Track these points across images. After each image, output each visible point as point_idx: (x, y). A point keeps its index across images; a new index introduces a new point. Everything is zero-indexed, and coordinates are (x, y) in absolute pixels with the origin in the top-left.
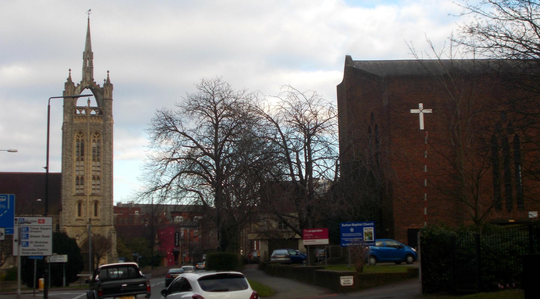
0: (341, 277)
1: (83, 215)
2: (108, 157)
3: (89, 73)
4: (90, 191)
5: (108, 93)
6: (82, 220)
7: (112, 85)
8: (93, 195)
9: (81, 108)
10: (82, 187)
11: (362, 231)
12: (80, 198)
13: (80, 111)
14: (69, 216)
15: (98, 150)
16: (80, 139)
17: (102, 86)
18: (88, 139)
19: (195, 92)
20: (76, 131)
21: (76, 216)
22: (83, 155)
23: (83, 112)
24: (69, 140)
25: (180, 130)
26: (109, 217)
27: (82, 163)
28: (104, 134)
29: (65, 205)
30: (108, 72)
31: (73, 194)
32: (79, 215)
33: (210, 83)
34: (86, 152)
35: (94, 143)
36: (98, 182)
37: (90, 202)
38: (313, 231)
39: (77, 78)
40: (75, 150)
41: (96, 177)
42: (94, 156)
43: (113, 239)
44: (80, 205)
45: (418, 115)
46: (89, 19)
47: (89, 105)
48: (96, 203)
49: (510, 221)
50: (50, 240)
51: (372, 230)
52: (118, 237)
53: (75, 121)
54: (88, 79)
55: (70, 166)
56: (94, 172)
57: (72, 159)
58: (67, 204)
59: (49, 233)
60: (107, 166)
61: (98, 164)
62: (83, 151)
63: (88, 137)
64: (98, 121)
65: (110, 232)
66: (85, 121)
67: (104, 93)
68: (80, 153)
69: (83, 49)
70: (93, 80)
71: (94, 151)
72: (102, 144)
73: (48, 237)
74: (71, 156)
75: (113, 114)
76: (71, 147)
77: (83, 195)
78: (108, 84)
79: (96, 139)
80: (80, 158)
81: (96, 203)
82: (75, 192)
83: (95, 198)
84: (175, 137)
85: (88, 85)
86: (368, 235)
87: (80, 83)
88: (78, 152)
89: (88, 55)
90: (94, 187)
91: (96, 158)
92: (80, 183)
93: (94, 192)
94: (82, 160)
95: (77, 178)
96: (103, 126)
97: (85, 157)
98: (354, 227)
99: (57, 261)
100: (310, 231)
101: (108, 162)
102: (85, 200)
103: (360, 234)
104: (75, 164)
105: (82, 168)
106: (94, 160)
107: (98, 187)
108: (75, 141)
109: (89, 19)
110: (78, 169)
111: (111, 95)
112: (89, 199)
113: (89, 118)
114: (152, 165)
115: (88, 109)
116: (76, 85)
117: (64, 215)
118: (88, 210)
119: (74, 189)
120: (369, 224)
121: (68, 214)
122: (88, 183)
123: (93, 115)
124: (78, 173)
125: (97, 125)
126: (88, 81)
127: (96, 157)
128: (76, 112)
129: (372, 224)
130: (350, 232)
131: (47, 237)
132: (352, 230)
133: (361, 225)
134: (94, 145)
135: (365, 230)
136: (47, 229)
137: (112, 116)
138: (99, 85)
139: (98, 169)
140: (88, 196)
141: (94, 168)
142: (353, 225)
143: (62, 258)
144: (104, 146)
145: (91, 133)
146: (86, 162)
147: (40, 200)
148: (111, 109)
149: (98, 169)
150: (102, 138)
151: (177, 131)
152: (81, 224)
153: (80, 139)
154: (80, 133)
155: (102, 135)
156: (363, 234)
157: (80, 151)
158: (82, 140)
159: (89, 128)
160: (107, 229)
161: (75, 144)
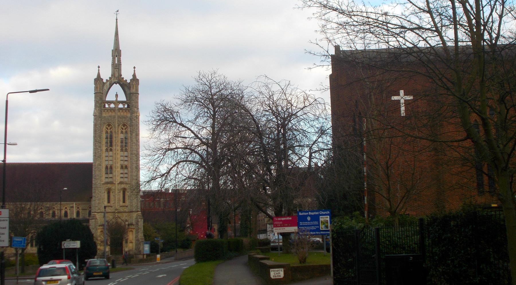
0: (271, 270)
1: (112, 202)
2: (134, 147)
4: (118, 179)
5: (135, 88)
6: (111, 207)
7: (138, 80)
8: (121, 183)
9: (110, 102)
10: (111, 176)
11: (318, 220)
12: (109, 186)
13: (109, 105)
14: (99, 203)
15: (125, 141)
16: (109, 131)
17: (129, 81)
18: (117, 131)
19: (193, 84)
20: (104, 123)
21: (106, 203)
22: (111, 145)
23: (112, 106)
25: (179, 121)
26: (135, 203)
27: (111, 153)
28: (131, 126)
29: (95, 192)
30: (134, 68)
31: (103, 183)
32: (109, 202)
33: (207, 75)
34: (114, 144)
35: (122, 135)
36: (126, 171)
37: (118, 190)
38: (283, 219)
39: (106, 74)
40: (104, 141)
41: (124, 166)
42: (122, 146)
43: (139, 224)
44: (109, 193)
45: (399, 101)
46: (117, 19)
47: (117, 99)
48: (124, 190)
49: (493, 205)
50: (6, 231)
51: (328, 218)
52: (144, 222)
53: (104, 115)
54: (117, 75)
55: (100, 157)
56: (122, 162)
57: (101, 150)
58: (97, 192)
59: (6, 224)
60: (134, 155)
61: (126, 154)
62: (111, 142)
63: (117, 129)
64: (125, 114)
65: (137, 218)
66: (113, 114)
67: (131, 88)
68: (109, 144)
69: (112, 47)
70: (121, 75)
71: (122, 142)
72: (129, 135)
73: (5, 228)
74: (100, 147)
75: (139, 107)
77: (112, 183)
78: (135, 79)
79: (124, 131)
81: (124, 190)
82: (104, 180)
83: (123, 186)
84: (175, 129)
85: (117, 80)
86: (324, 224)
87: (108, 79)
88: (107, 143)
89: (117, 53)
90: (122, 176)
91: (124, 149)
92: (109, 172)
93: (122, 180)
94: (111, 150)
95: (107, 168)
96: (131, 119)
97: (114, 148)
98: (311, 216)
99: (71, 247)
100: (279, 219)
101: (135, 152)
102: (113, 187)
103: (316, 223)
104: (104, 154)
105: (111, 158)
106: (122, 150)
107: (126, 176)
108: (104, 132)
109: (117, 19)
111: (137, 90)
112: (117, 188)
113: (116, 111)
114: (150, 155)
115: (117, 102)
116: (105, 81)
117: (95, 202)
118: (117, 196)
119: (104, 178)
120: (325, 213)
121: (97, 202)
122: (117, 172)
123: (121, 109)
124: (107, 163)
125: (125, 118)
126: (117, 78)
127: (124, 147)
128: (105, 106)
129: (328, 212)
130: (307, 221)
131: (4, 228)
132: (309, 218)
133: (317, 213)
134: (122, 136)
135: (322, 219)
136: (4, 220)
137: (138, 109)
138: (126, 80)
139: (126, 159)
140: (117, 185)
141: (122, 158)
142: (310, 213)
143: (75, 244)
144: (131, 138)
145: (119, 125)
147: (66, 189)
148: (137, 102)
149: (126, 159)
150: (129, 130)
151: (175, 122)
152: (110, 211)
153: (109, 131)
154: (109, 125)
155: (129, 127)
156: (319, 223)
158: (111, 132)
160: (135, 215)
161: (104, 135)
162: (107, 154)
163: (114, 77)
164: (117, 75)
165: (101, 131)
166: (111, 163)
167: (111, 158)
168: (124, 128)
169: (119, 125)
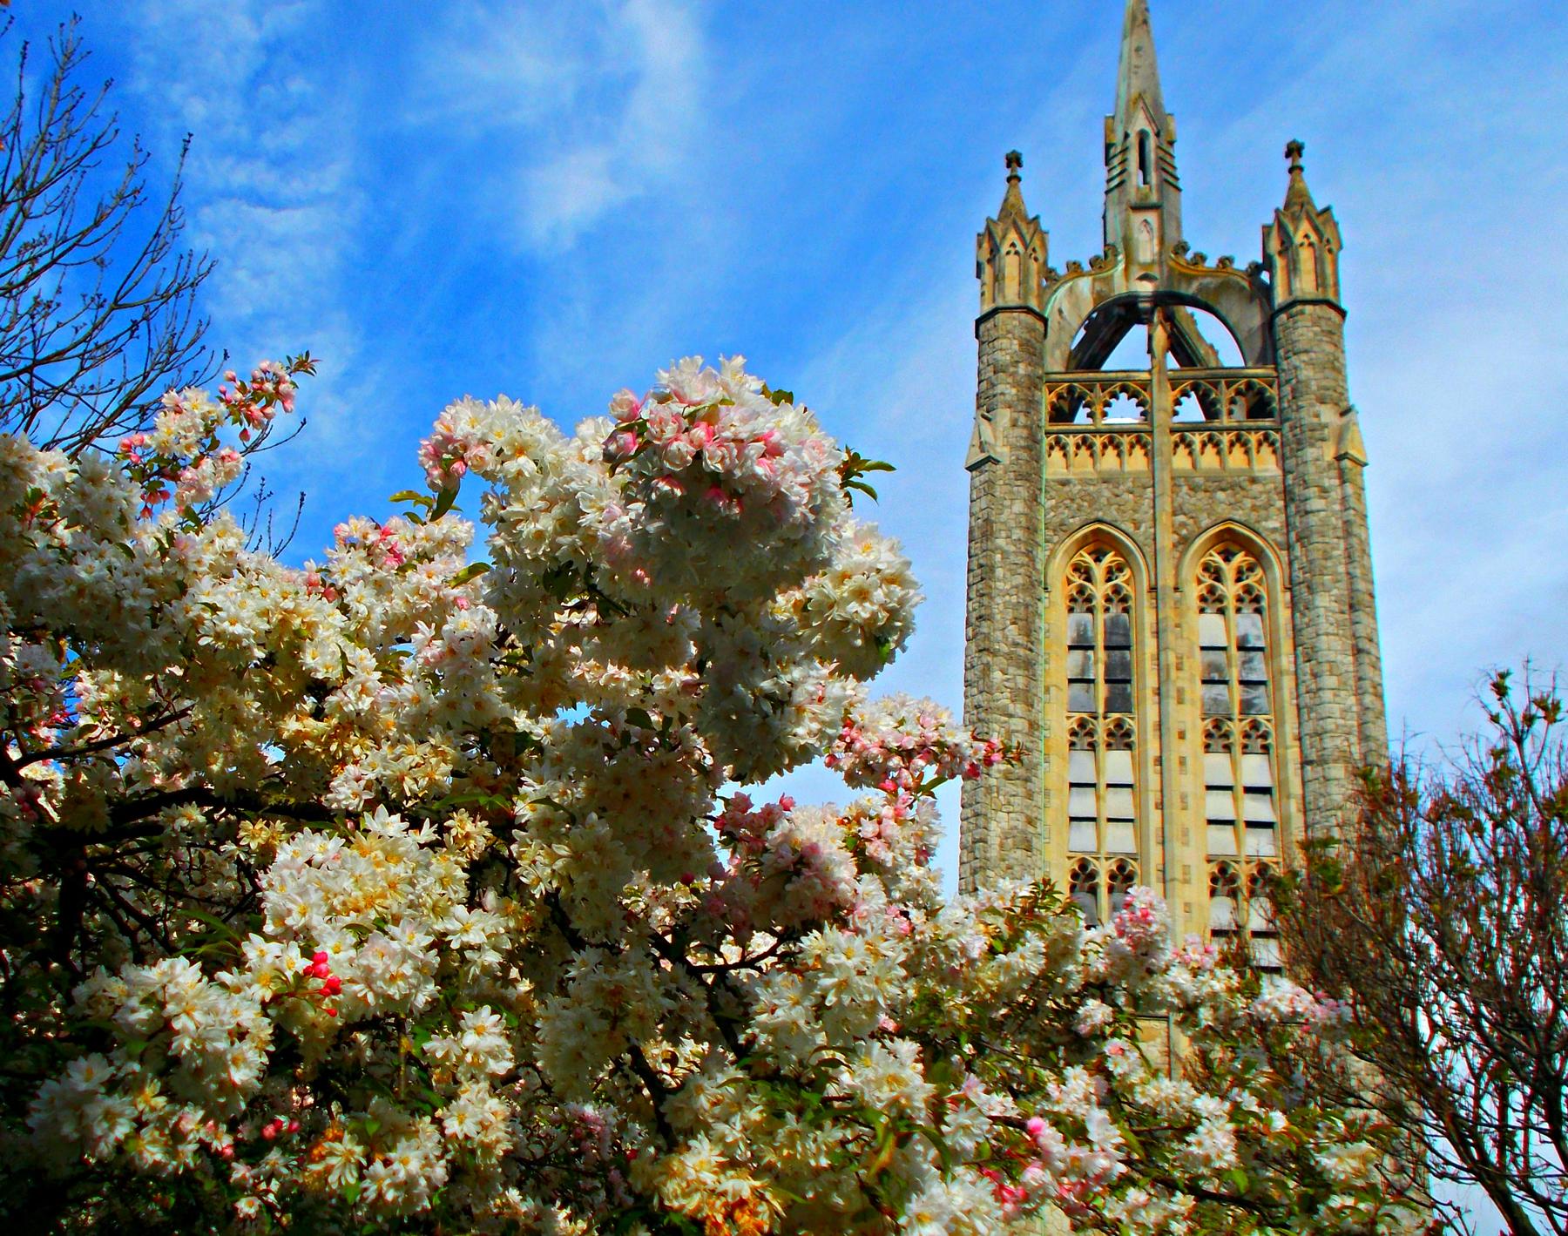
2: (1338, 706)
3: (1152, 217)
16: (1100, 590)
18: (1167, 580)
20: (1062, 528)
22: (1120, 700)
24: (1005, 581)
27: (1118, 764)
28: (1297, 536)
30: (1294, 150)
40: (1060, 664)
53: (1054, 466)
57: (1033, 726)
61: (1255, 769)
62: (1119, 679)
64: (1236, 459)
66: (1137, 461)
68: (1102, 690)
70: (1182, 248)
72: (1284, 614)
74: (1026, 697)
76: (1029, 632)
79: (1230, 589)
80: (1101, 728)
91: (1236, 727)
94: (1121, 737)
96: (1287, 494)
104: (1060, 765)
105: (1120, 804)
106: (1216, 737)
108: (1059, 594)
110: (1083, 804)
124: (1083, 839)
139: (1258, 809)
141: (1221, 805)
146: (1153, 749)
149: (1258, 809)
150: (1278, 572)
153: (1100, 590)
157: (1099, 673)
158: (1118, 596)
159: (1165, 505)
161: (1058, 622)
162: (1082, 766)
163: (1129, 261)
164: (1147, 250)
165: (1035, 585)
166: (1120, 840)
167: (1120, 804)
168: (1229, 570)
169: (1184, 542)
